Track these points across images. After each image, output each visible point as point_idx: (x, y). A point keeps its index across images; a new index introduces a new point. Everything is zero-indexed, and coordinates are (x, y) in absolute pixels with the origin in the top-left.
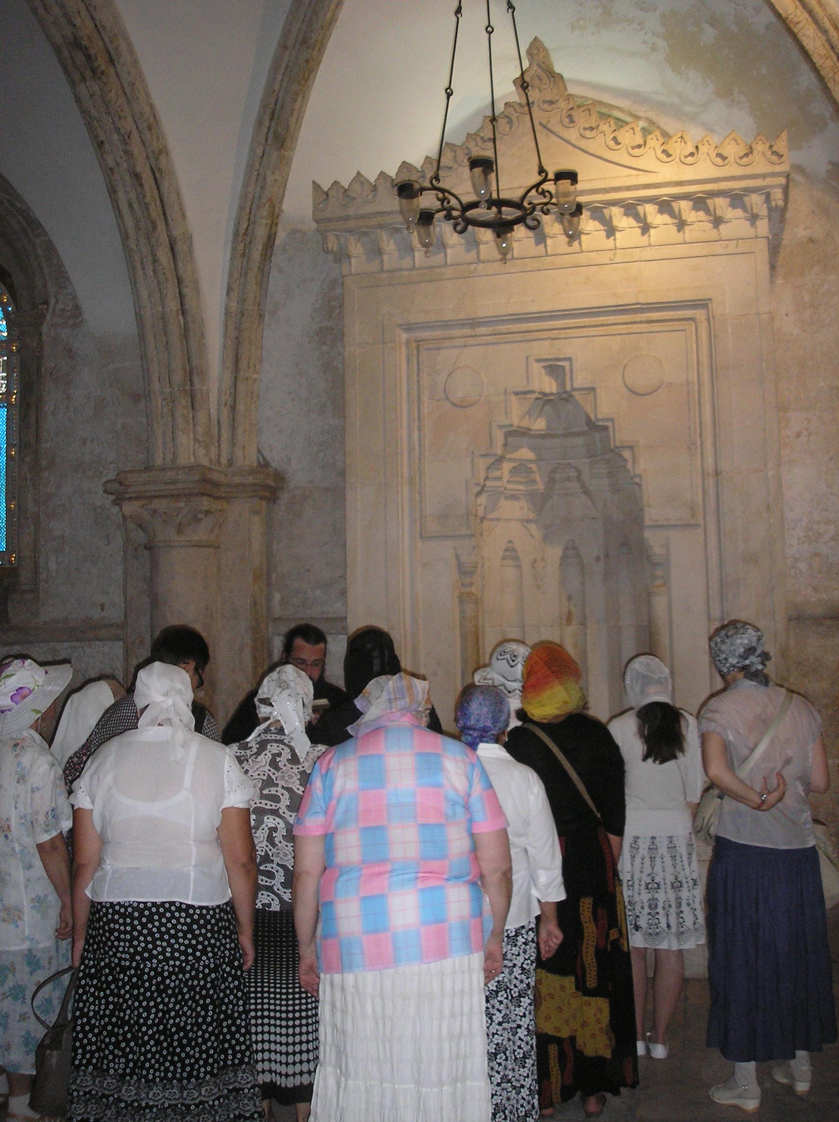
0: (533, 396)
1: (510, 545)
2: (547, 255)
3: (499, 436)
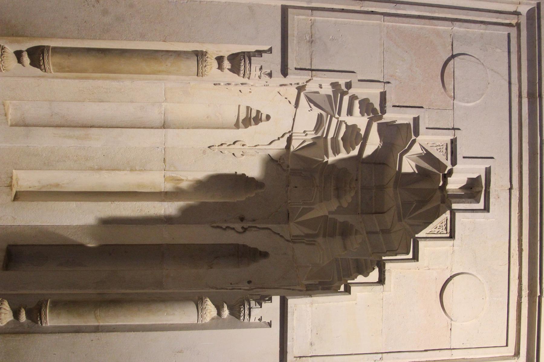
0: (448, 163)
1: (264, 117)
3: (403, 117)
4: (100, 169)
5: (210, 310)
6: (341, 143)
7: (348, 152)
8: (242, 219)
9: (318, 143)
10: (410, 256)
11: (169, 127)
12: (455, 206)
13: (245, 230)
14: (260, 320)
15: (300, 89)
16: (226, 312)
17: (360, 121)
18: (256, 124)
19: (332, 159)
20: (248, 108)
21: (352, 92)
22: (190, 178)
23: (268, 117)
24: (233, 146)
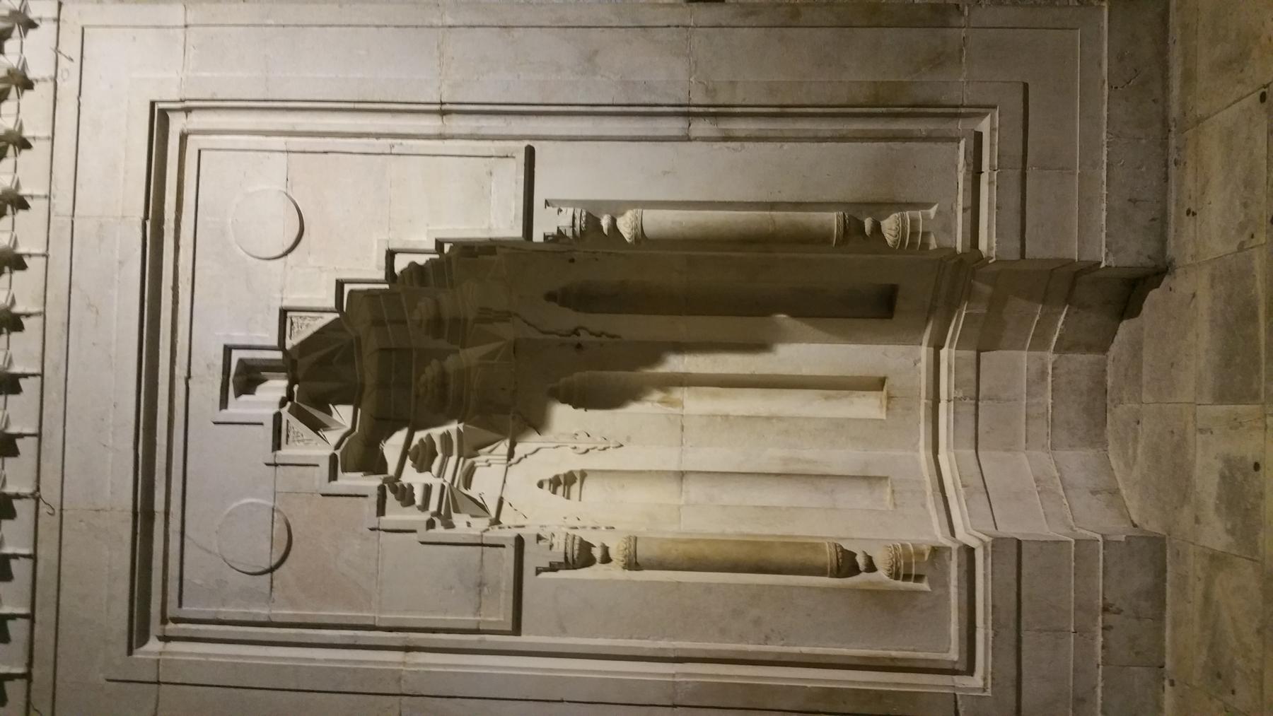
1: (546, 485)
2: (42, 375)
3: (352, 481)
4: (769, 419)
5: (625, 226)
6: (438, 448)
7: (429, 436)
8: (579, 346)
9: (470, 449)
10: (347, 288)
11: (675, 473)
12: (278, 355)
13: (576, 332)
14: (560, 210)
15: (496, 522)
16: (605, 222)
17: (411, 476)
18: (557, 477)
19: (453, 427)
20: (568, 498)
21: (426, 516)
22: (648, 405)
23: (541, 485)
24: (590, 446)
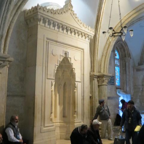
5: (75, 91)
8: (59, 85)
13: (61, 85)
16: (76, 89)
